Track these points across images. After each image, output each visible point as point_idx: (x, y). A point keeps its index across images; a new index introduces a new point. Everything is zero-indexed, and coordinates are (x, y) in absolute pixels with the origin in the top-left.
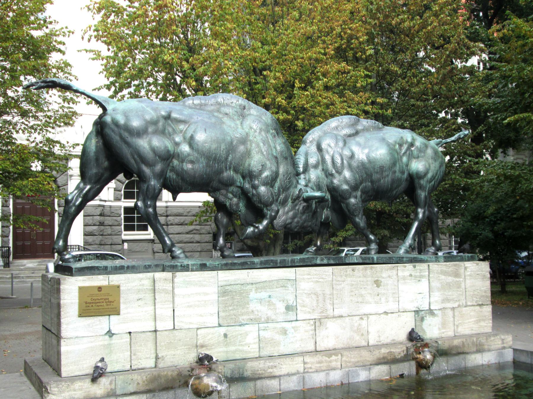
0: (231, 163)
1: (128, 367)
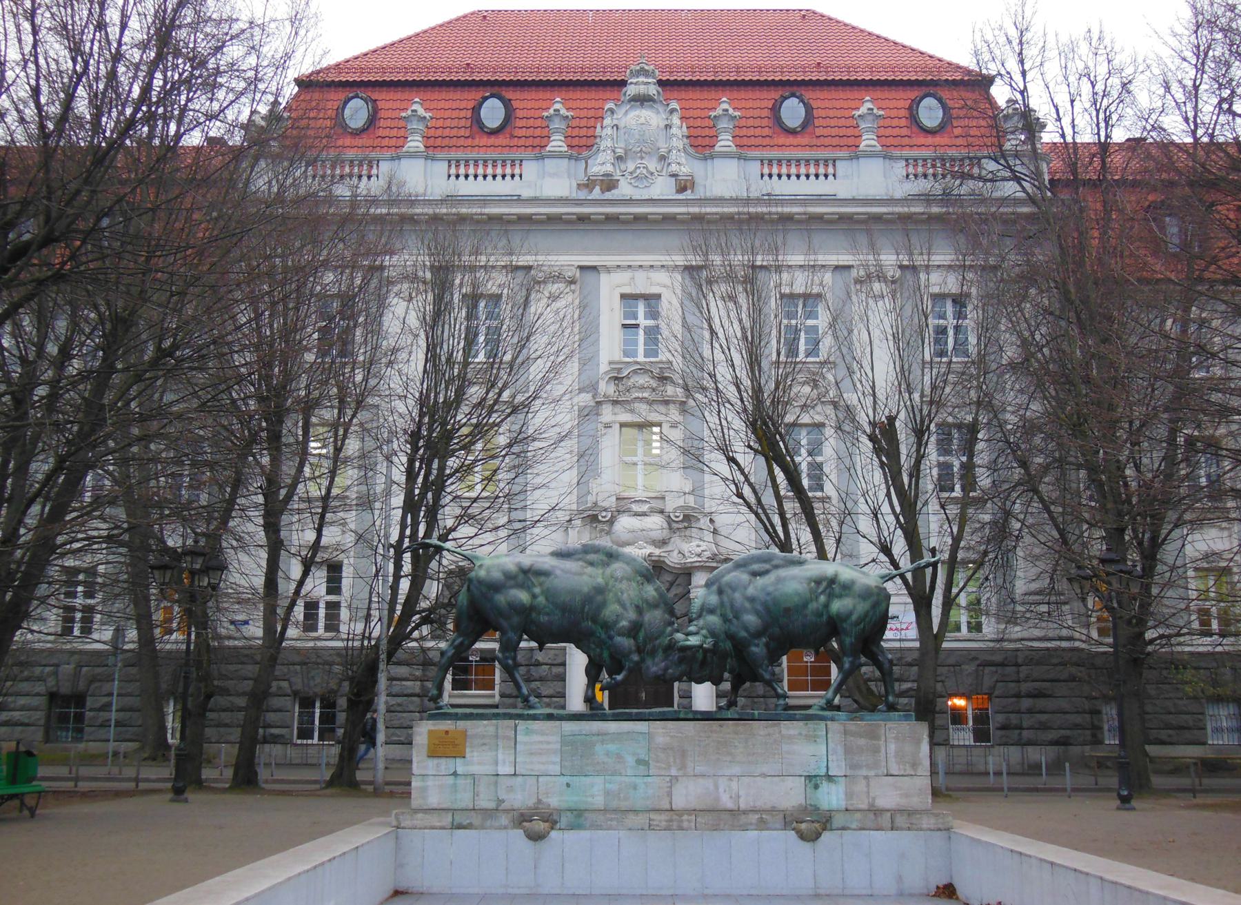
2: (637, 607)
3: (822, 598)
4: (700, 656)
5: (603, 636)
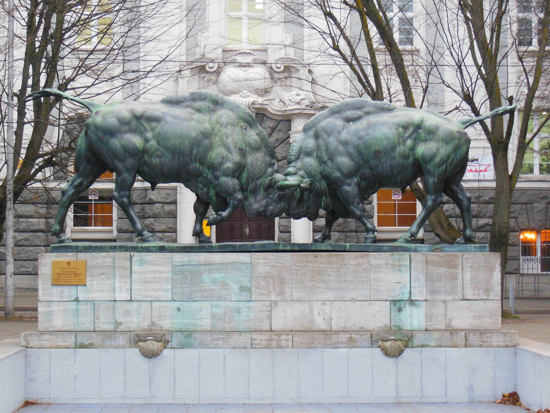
0: (196, 157)
1: (92, 329)
2: (241, 149)
3: (409, 142)
4: (297, 194)
5: (210, 176)
